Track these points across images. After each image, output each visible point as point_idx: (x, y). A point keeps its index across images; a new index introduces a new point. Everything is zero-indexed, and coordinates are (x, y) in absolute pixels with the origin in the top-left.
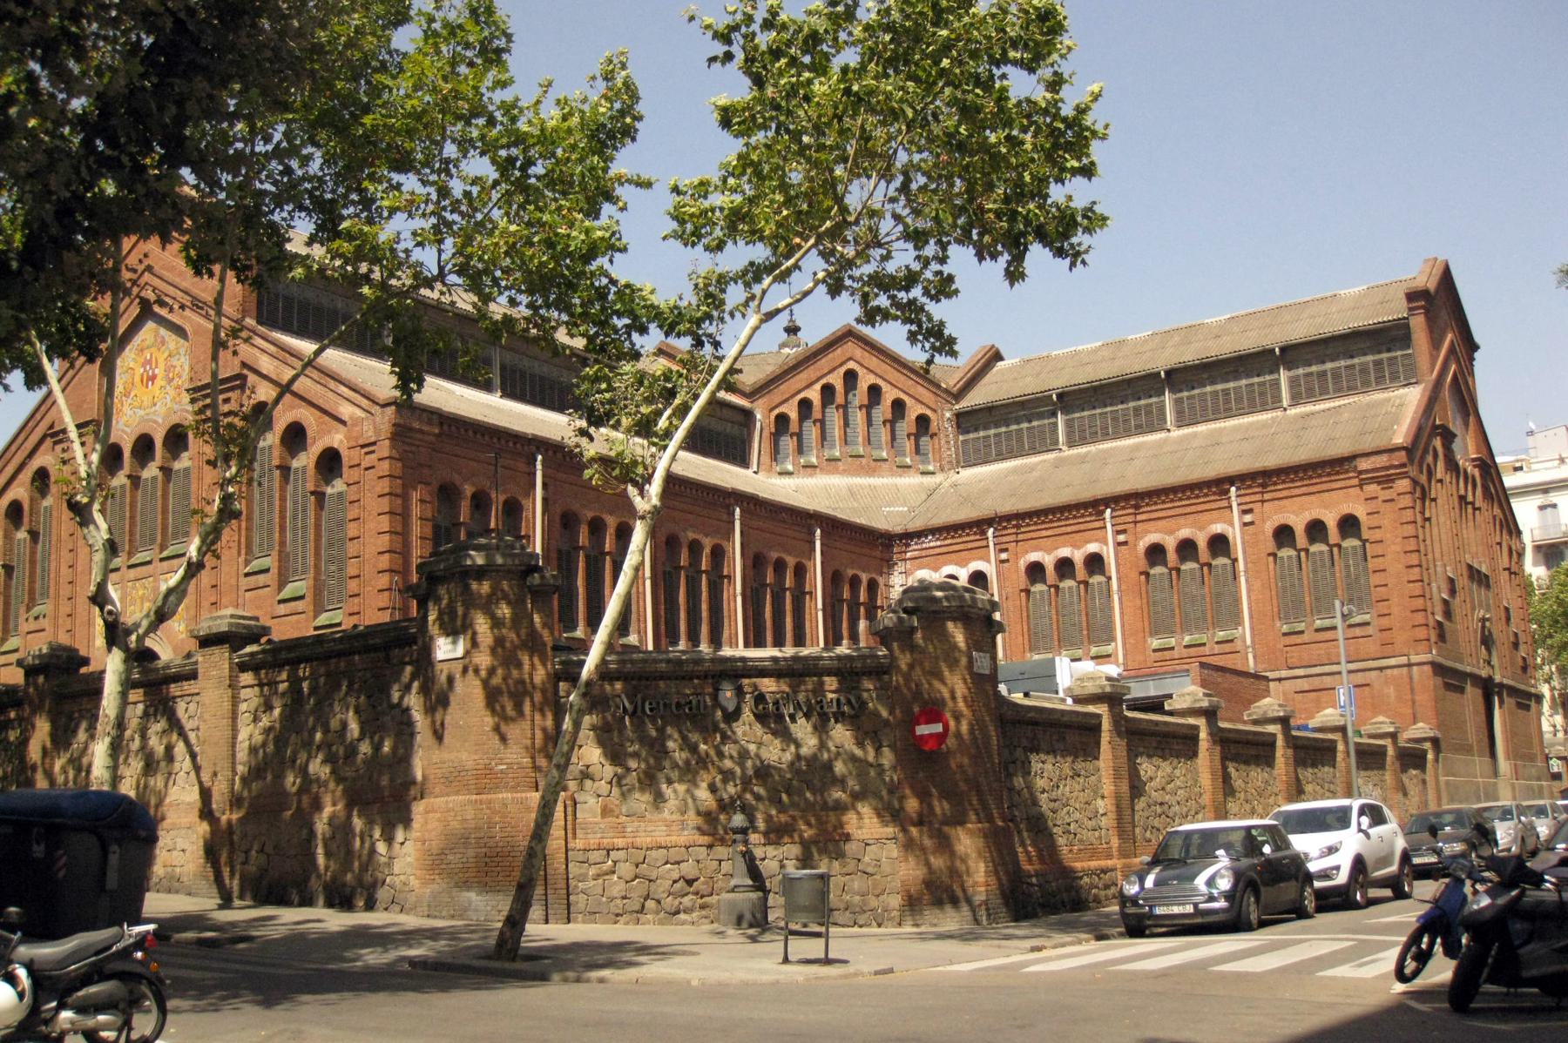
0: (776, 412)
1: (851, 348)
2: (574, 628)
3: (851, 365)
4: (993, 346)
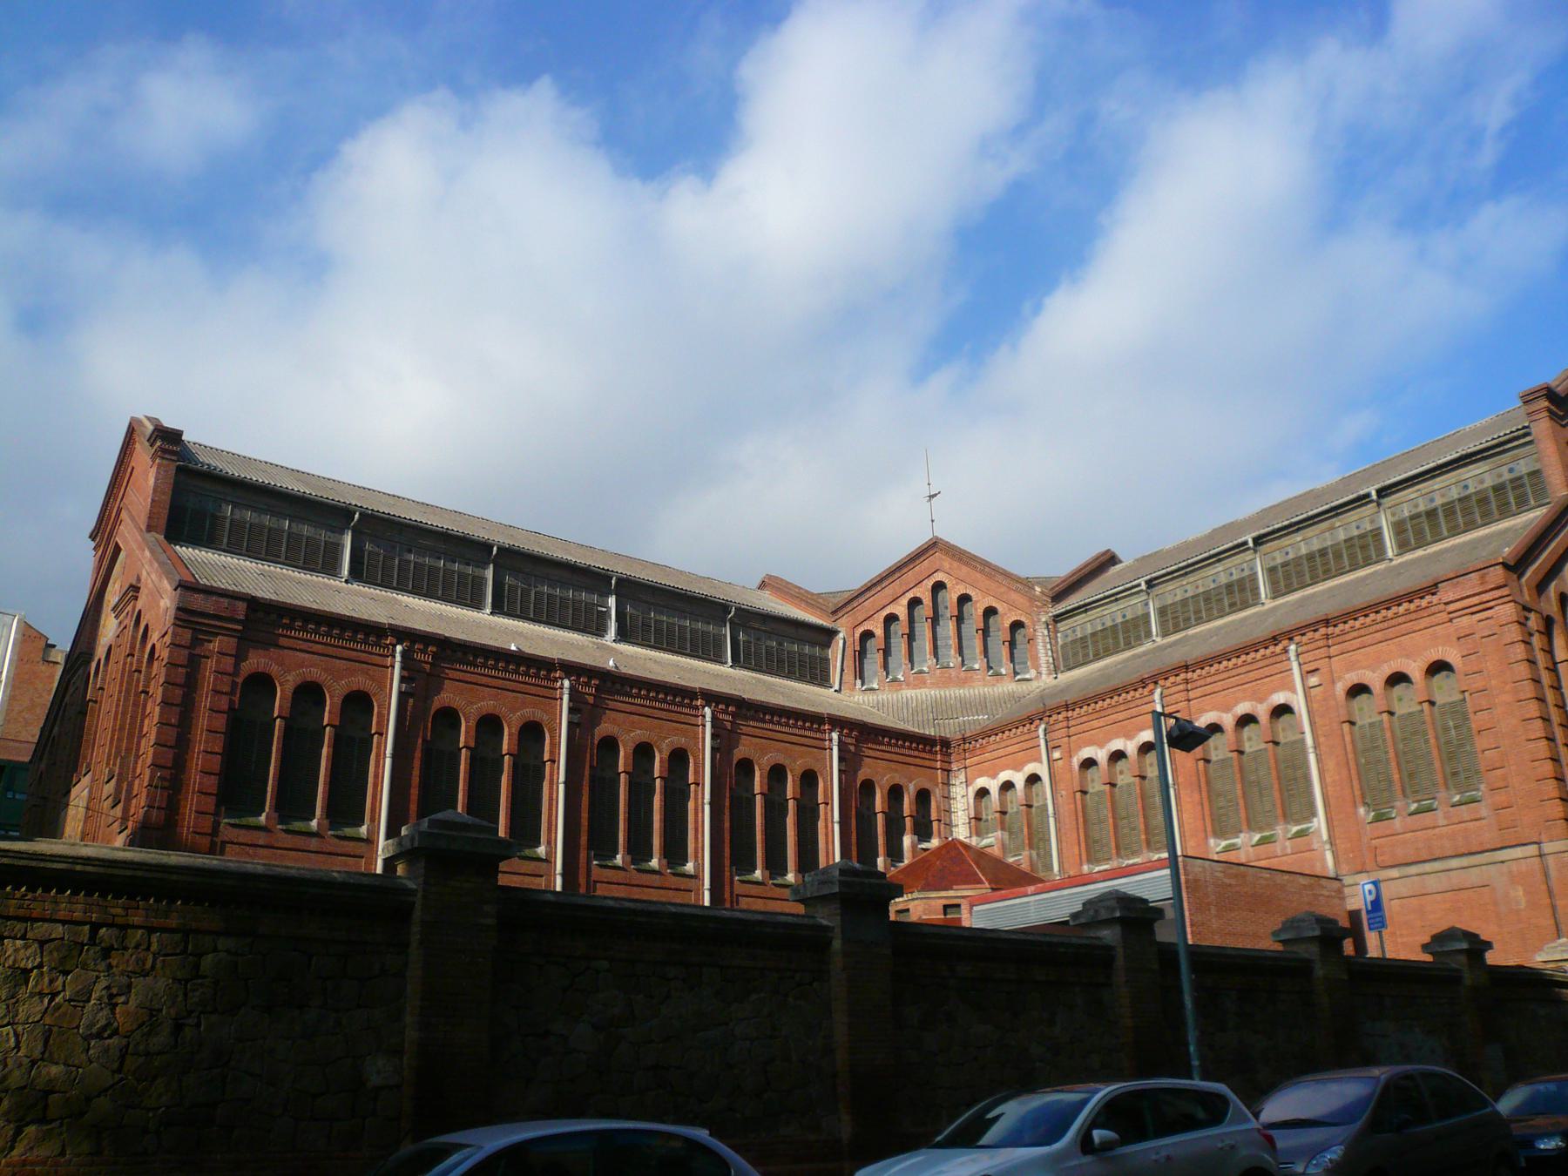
0: (860, 630)
1: (938, 558)
2: (784, 872)
3: (939, 577)
4: (1109, 550)
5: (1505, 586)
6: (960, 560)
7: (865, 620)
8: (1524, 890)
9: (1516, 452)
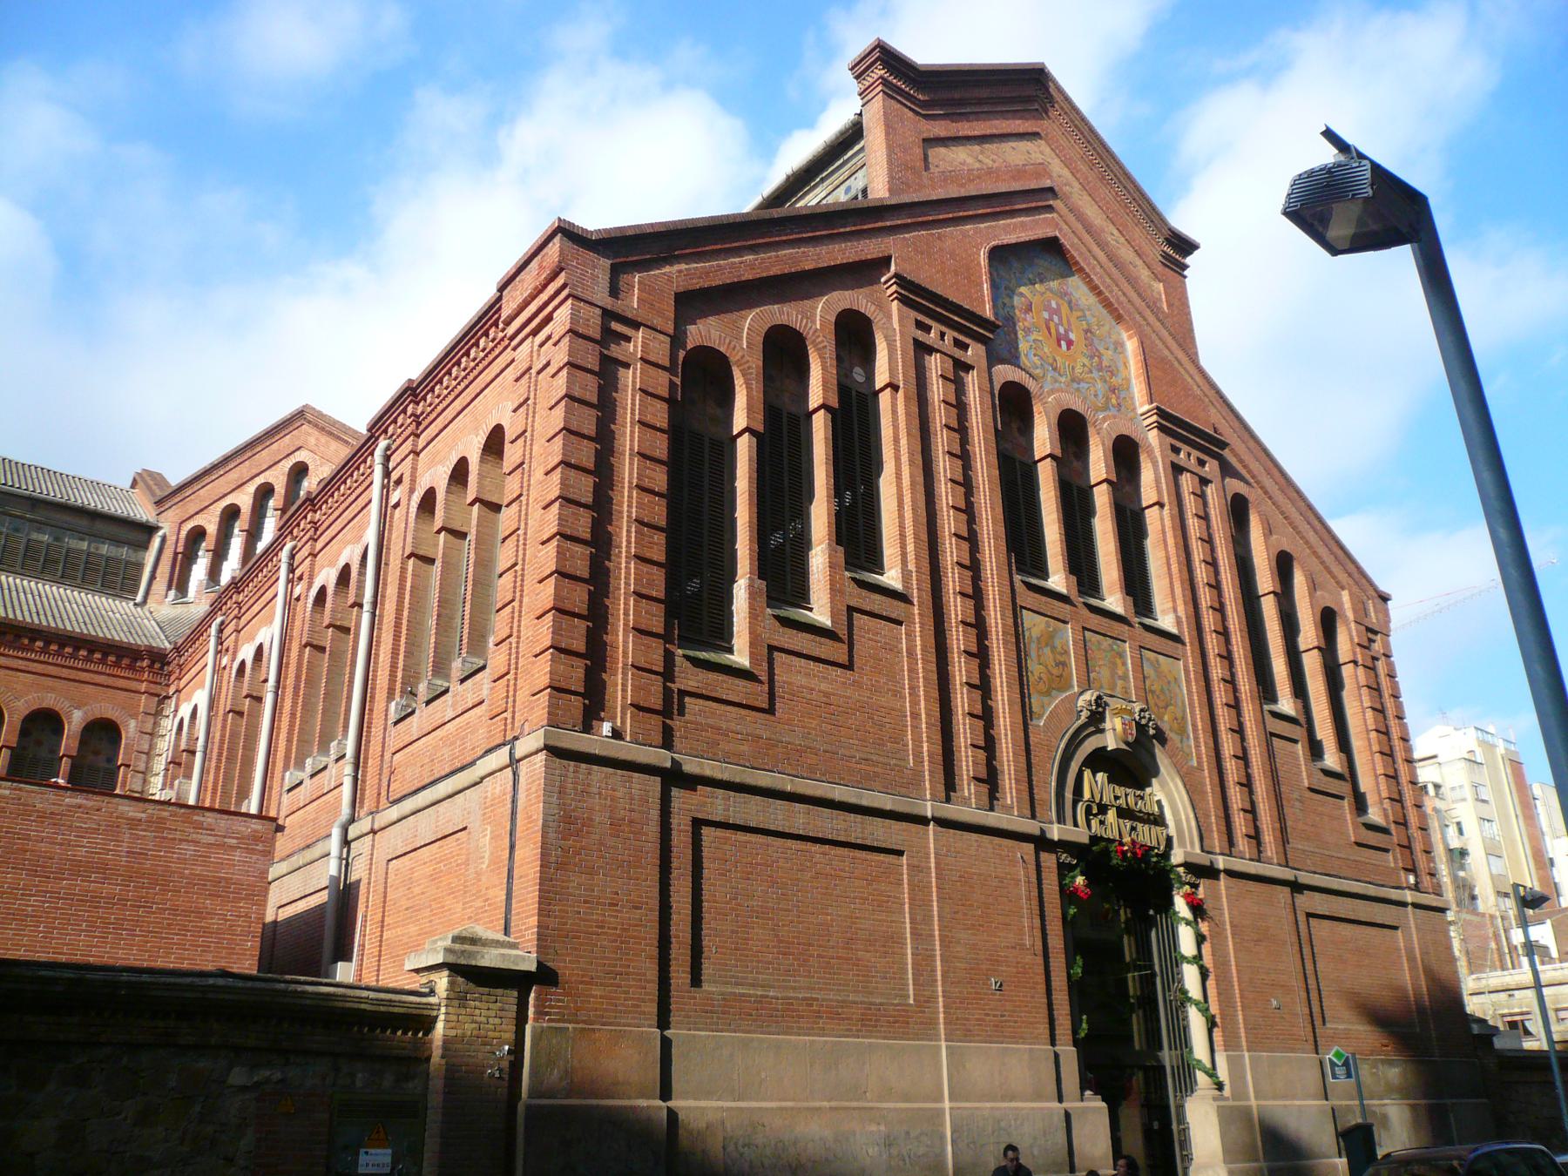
5: (562, 269)
6: (330, 434)
7: (197, 513)
8: (491, 832)
9: (852, 163)
